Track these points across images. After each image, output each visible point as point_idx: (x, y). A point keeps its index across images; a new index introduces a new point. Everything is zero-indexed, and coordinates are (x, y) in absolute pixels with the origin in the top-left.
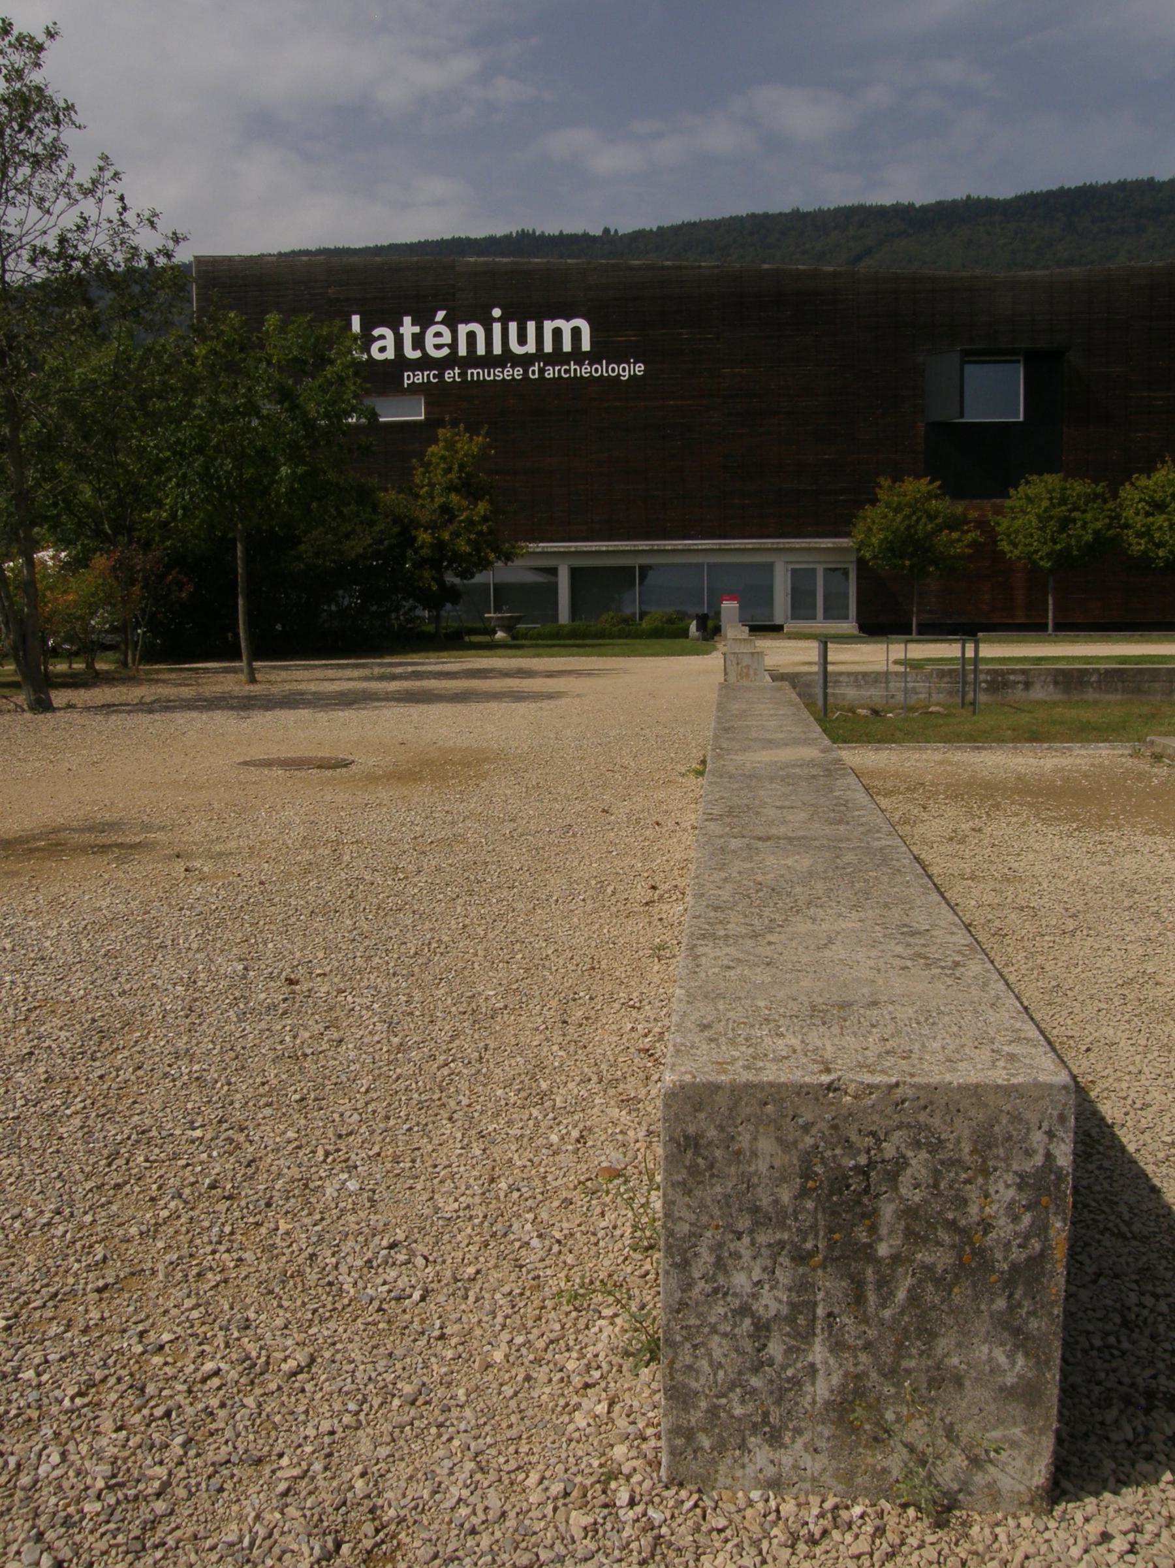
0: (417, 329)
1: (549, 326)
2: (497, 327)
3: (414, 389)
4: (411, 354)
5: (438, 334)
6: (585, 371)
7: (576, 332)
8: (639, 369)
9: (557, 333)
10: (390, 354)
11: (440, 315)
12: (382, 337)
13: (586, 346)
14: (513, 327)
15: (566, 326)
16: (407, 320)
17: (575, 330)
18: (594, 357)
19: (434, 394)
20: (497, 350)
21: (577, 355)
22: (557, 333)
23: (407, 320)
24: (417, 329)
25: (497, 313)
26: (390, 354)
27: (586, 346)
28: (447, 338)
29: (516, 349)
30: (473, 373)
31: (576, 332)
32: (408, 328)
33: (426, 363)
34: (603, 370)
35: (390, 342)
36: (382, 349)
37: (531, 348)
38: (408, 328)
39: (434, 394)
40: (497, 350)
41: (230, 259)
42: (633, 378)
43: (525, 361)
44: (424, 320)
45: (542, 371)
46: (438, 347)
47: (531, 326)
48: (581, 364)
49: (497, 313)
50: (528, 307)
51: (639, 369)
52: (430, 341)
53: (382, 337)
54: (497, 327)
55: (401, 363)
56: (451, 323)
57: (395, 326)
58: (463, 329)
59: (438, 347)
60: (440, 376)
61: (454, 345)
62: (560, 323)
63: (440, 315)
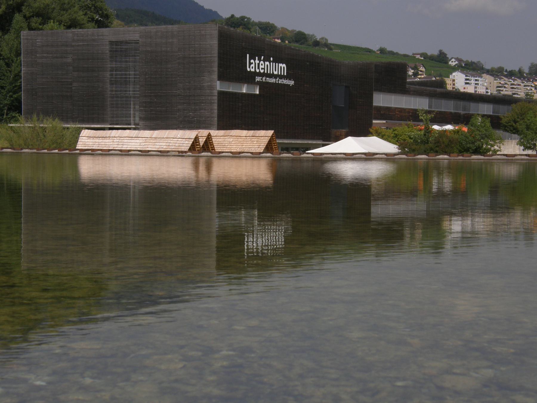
1: (280, 65)
3: (259, 83)
4: (258, 71)
7: (284, 67)
9: (281, 67)
10: (253, 70)
11: (263, 57)
16: (257, 58)
19: (260, 84)
22: (281, 67)
23: (257, 58)
24: (258, 62)
25: (272, 59)
31: (284, 67)
32: (257, 62)
33: (260, 74)
35: (253, 65)
36: (252, 68)
43: (276, 76)
46: (262, 69)
49: (272, 59)
52: (261, 67)
53: (252, 63)
55: (256, 74)
57: (255, 60)
60: (262, 79)
61: (264, 69)
63: (263, 57)
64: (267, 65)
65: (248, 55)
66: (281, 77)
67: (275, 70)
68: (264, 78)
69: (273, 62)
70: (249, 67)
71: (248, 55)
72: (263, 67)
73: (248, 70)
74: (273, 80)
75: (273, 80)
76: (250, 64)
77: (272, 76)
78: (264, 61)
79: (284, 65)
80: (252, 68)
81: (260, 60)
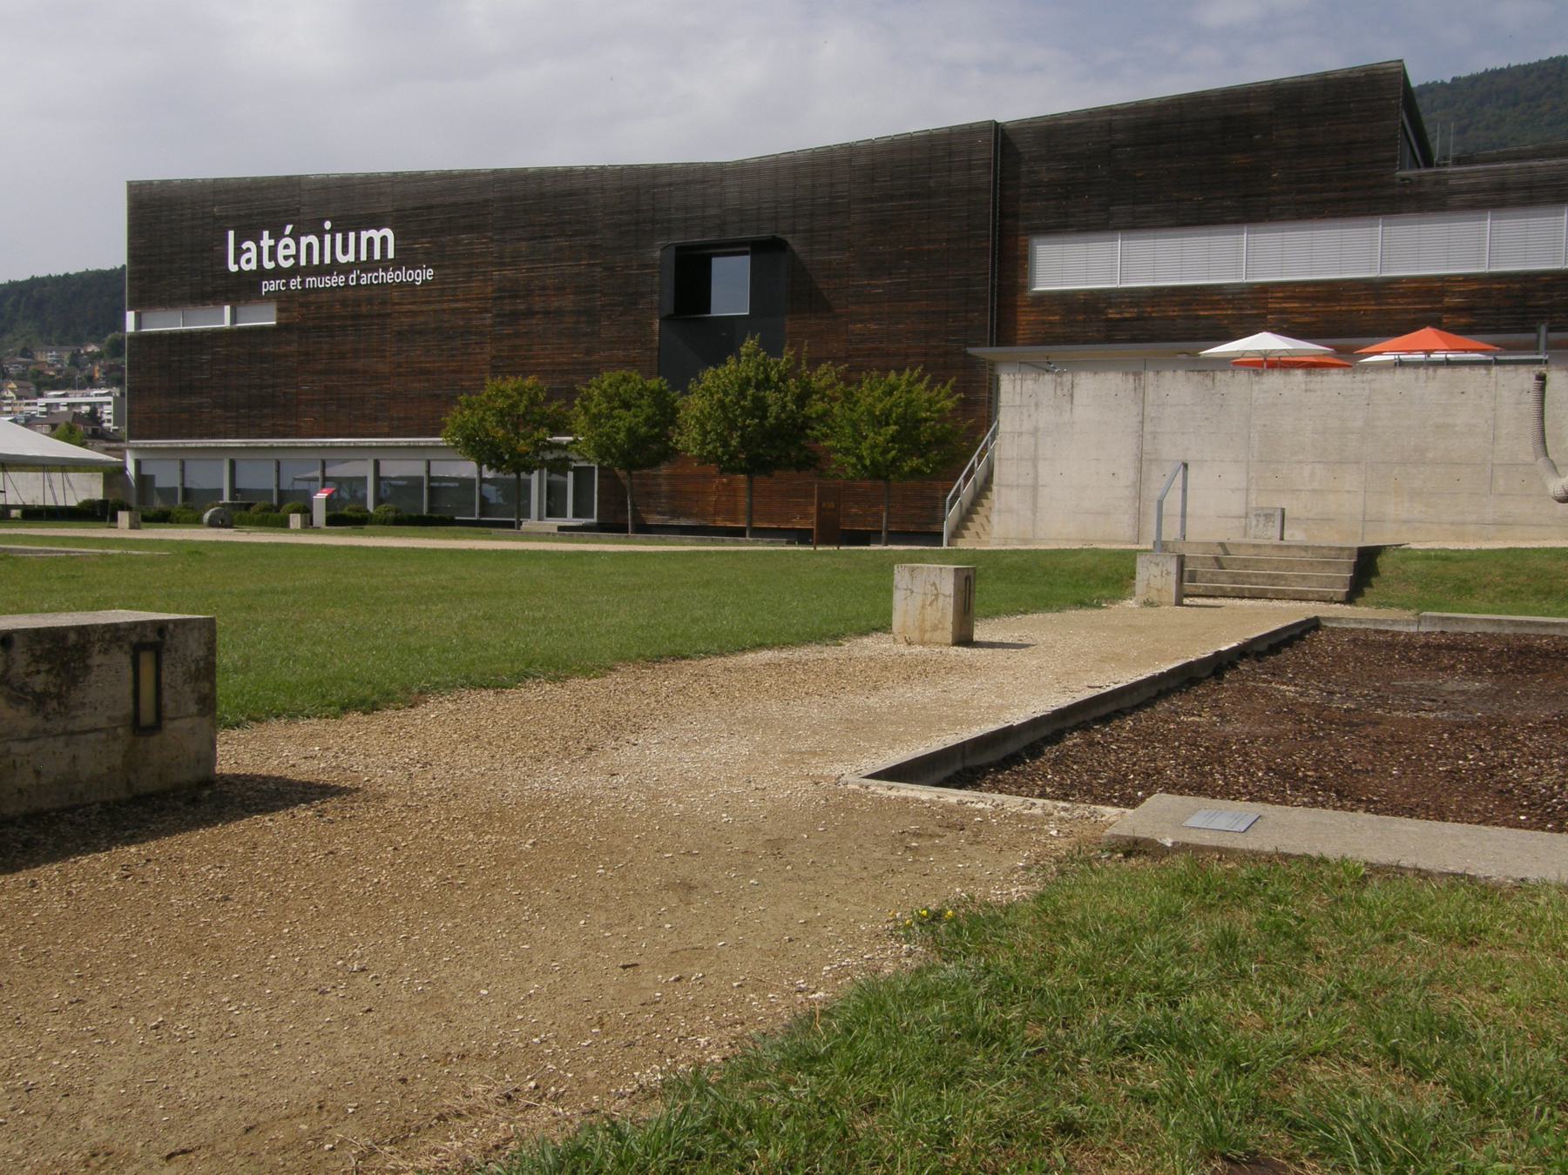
0: (272, 242)
1: (365, 235)
2: (328, 238)
4: (269, 265)
5: (287, 247)
6: (390, 277)
7: (384, 240)
8: (429, 274)
9: (370, 241)
10: (253, 266)
11: (289, 228)
12: (249, 250)
13: (391, 255)
14: (339, 237)
15: (376, 235)
16: (266, 234)
17: (382, 238)
18: (397, 264)
19: (283, 300)
20: (327, 260)
21: (384, 264)
22: (370, 241)
23: (266, 234)
24: (272, 242)
25: (328, 225)
26: (253, 266)
27: (391, 255)
28: (292, 251)
29: (342, 259)
30: (311, 281)
31: (384, 240)
32: (266, 242)
33: (278, 273)
34: (403, 276)
35: (253, 255)
36: (248, 261)
37: (351, 257)
38: (266, 242)
39: (283, 300)
40: (327, 260)
41: (150, 183)
42: (425, 282)
43: (346, 269)
44: (277, 235)
45: (358, 278)
46: (286, 258)
47: (352, 235)
48: (386, 270)
49: (328, 225)
50: (350, 223)
51: (429, 274)
52: (281, 252)
53: (249, 250)
54: (328, 238)
55: (261, 273)
56: (295, 236)
57: (257, 240)
58: (304, 241)
59: (286, 258)
60: (287, 285)
61: (297, 257)
62: (373, 233)
63: (289, 228)
64: (309, 246)
65: (231, 234)
66: (370, 266)
67: (345, 251)
68: (295, 283)
69: (333, 232)
70: (237, 261)
71: (231, 234)
72: (292, 251)
73: (233, 268)
74: (337, 280)
75: (337, 280)
76: (239, 252)
77: (335, 268)
78: (295, 236)
79: (388, 232)
80: (248, 261)
81: (277, 235)
